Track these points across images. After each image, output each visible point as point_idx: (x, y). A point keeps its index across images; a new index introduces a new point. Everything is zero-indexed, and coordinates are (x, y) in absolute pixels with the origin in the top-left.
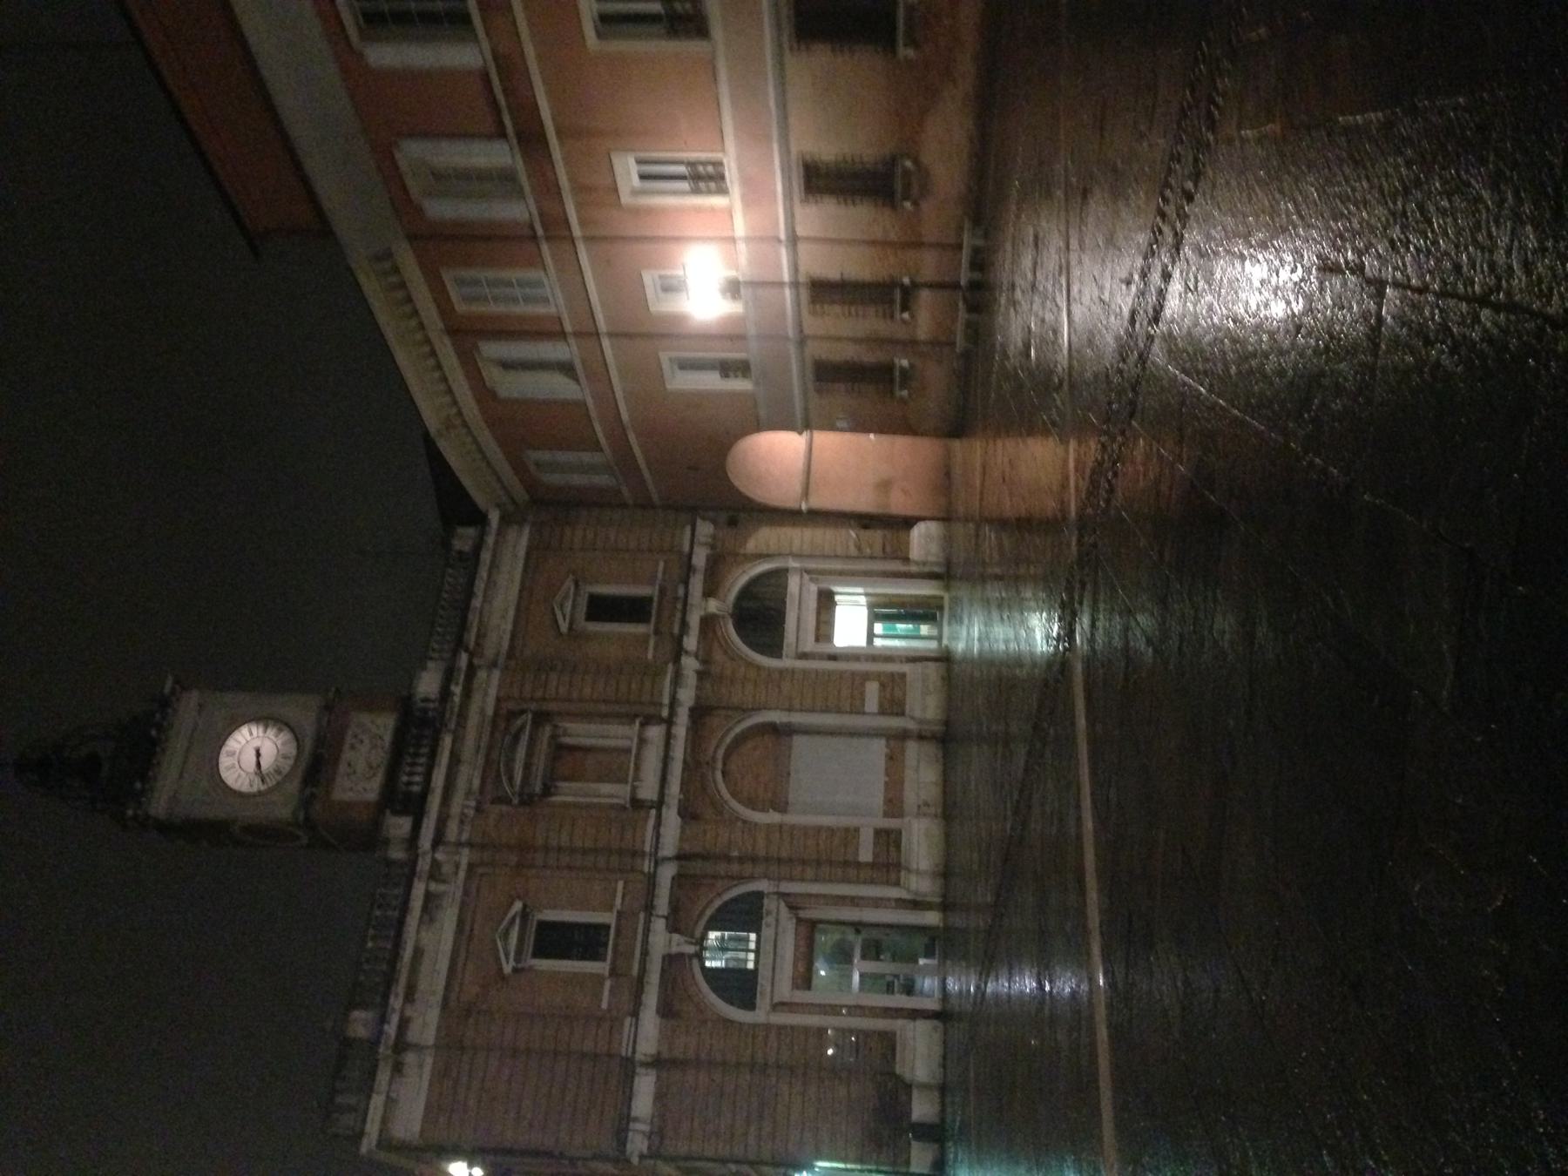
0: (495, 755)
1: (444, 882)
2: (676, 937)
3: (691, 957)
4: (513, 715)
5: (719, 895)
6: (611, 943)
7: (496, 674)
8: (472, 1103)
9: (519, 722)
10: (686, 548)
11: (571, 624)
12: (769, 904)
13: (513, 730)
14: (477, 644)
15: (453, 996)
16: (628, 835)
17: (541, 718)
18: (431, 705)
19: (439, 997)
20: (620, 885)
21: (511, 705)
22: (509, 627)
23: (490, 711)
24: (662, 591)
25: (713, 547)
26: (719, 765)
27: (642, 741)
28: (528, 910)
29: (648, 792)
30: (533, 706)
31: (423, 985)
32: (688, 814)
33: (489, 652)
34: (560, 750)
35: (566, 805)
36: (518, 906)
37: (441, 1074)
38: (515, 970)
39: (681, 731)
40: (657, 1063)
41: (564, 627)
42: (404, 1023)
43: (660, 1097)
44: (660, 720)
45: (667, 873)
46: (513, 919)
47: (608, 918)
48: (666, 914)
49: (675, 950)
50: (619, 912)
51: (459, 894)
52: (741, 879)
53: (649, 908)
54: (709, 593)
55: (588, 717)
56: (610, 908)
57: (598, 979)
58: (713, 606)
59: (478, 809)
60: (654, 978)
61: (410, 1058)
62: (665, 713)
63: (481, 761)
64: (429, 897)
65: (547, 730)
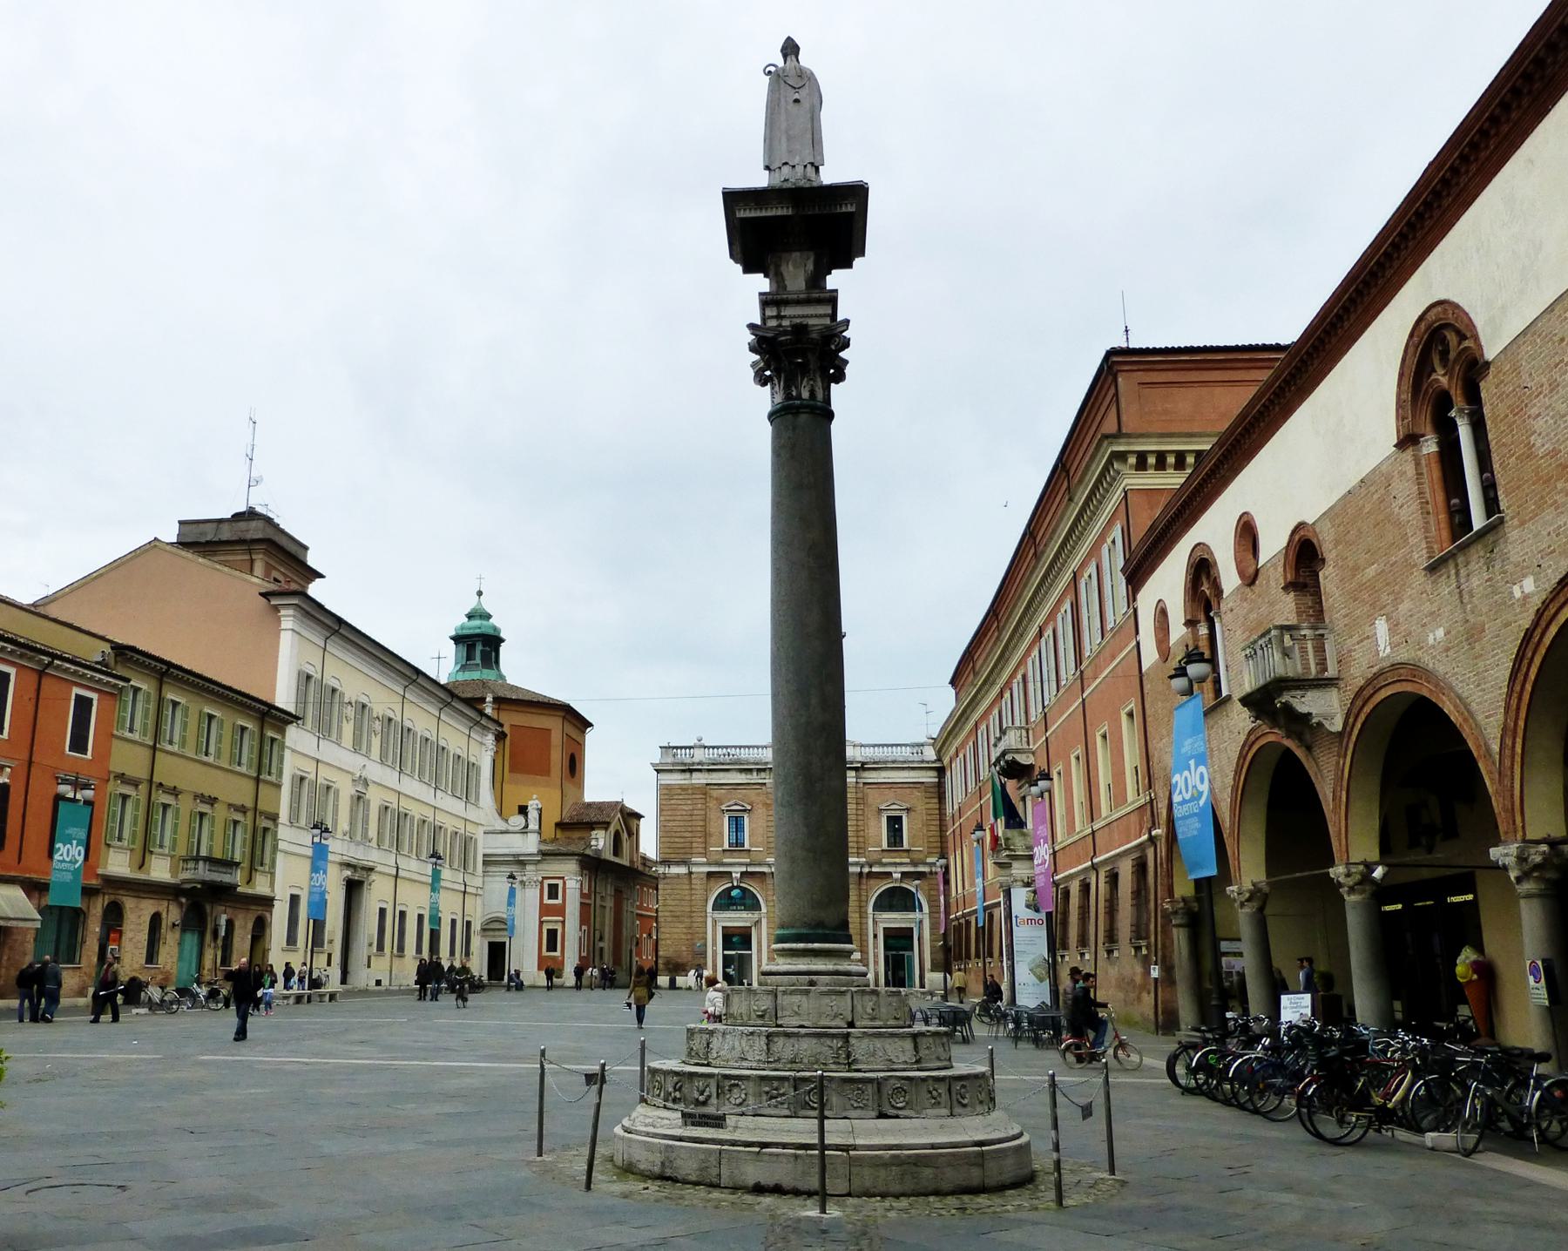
2: (739, 875)
8: (672, 802)
10: (929, 860)
12: (755, 916)
19: (710, 782)
22: (880, 781)
24: (908, 851)
25: (931, 873)
31: (715, 775)
33: (866, 774)
37: (683, 788)
40: (691, 873)
42: (700, 770)
43: (678, 875)
47: (747, 846)
49: (734, 875)
50: (749, 851)
51: (752, 782)
54: (903, 874)
58: (898, 876)
60: (722, 869)
61: (687, 775)
64: (750, 770)
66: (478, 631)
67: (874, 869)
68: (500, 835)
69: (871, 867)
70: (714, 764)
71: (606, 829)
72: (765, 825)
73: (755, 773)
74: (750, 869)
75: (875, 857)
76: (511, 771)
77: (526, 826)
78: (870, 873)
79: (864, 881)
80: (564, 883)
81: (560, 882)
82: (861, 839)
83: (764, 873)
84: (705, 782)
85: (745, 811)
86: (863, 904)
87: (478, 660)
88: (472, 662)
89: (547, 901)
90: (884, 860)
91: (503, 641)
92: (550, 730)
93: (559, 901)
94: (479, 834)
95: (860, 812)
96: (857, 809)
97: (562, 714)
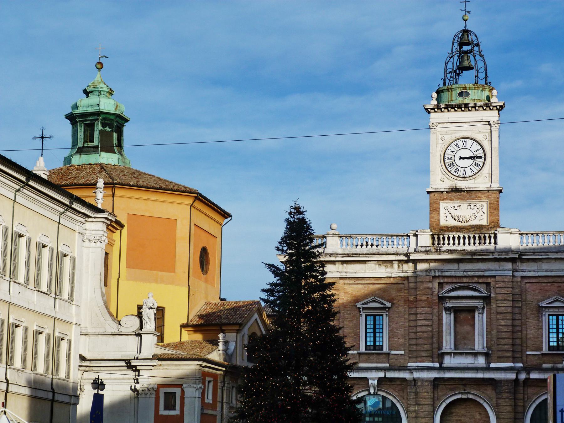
0: (465, 280)
1: (399, 267)
2: (376, 382)
3: (369, 390)
4: (488, 284)
5: (399, 401)
6: (373, 352)
7: (511, 273)
9: (482, 288)
11: (545, 307)
13: (478, 286)
14: (528, 260)
15: (347, 281)
16: (424, 354)
17: (487, 300)
18: (493, 241)
19: (344, 275)
20: (403, 352)
21: (492, 284)
22: (541, 274)
23: (487, 274)
26: (464, 396)
27: (476, 355)
28: (387, 309)
29: (448, 361)
30: (492, 295)
31: (350, 267)
32: (436, 382)
34: (471, 310)
35: (440, 320)
36: (389, 305)
38: (359, 308)
39: (480, 375)
41: (544, 305)
42: (333, 262)
44: (488, 362)
45: (406, 375)
46: (382, 303)
47: (386, 349)
48: (387, 377)
49: (370, 382)
50: (389, 354)
52: (407, 412)
53: (391, 369)
55: (489, 323)
56: (390, 349)
57: (358, 348)
59: (434, 277)
62: (492, 365)
63: (461, 274)
64: (391, 262)
65: (479, 304)
66: (96, 109)
67: (534, 376)
68: (111, 337)
69: (528, 373)
70: (348, 255)
71: (238, 331)
72: (407, 324)
73: (396, 265)
74: (390, 375)
75: (535, 362)
76: (128, 266)
77: (141, 327)
78: (527, 380)
79: (521, 389)
80: (183, 392)
81: (178, 391)
82: (518, 341)
83: (404, 379)
84: (339, 275)
85: (384, 308)
86: (520, 416)
87: (96, 142)
88: (90, 144)
89: (162, 412)
90: (544, 366)
91: (127, 121)
92: (176, 219)
93: (177, 412)
94: (73, 334)
95: (517, 310)
96: (513, 307)
97: (190, 201)
